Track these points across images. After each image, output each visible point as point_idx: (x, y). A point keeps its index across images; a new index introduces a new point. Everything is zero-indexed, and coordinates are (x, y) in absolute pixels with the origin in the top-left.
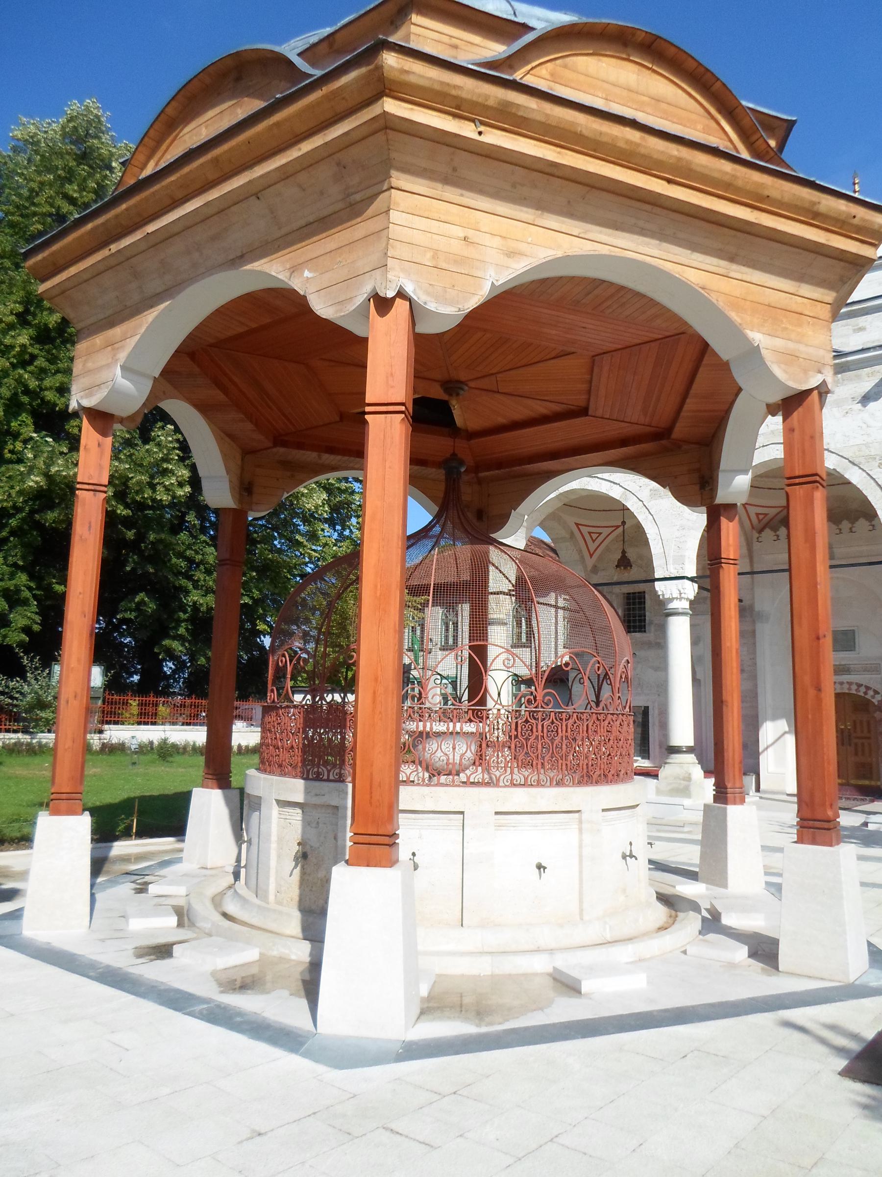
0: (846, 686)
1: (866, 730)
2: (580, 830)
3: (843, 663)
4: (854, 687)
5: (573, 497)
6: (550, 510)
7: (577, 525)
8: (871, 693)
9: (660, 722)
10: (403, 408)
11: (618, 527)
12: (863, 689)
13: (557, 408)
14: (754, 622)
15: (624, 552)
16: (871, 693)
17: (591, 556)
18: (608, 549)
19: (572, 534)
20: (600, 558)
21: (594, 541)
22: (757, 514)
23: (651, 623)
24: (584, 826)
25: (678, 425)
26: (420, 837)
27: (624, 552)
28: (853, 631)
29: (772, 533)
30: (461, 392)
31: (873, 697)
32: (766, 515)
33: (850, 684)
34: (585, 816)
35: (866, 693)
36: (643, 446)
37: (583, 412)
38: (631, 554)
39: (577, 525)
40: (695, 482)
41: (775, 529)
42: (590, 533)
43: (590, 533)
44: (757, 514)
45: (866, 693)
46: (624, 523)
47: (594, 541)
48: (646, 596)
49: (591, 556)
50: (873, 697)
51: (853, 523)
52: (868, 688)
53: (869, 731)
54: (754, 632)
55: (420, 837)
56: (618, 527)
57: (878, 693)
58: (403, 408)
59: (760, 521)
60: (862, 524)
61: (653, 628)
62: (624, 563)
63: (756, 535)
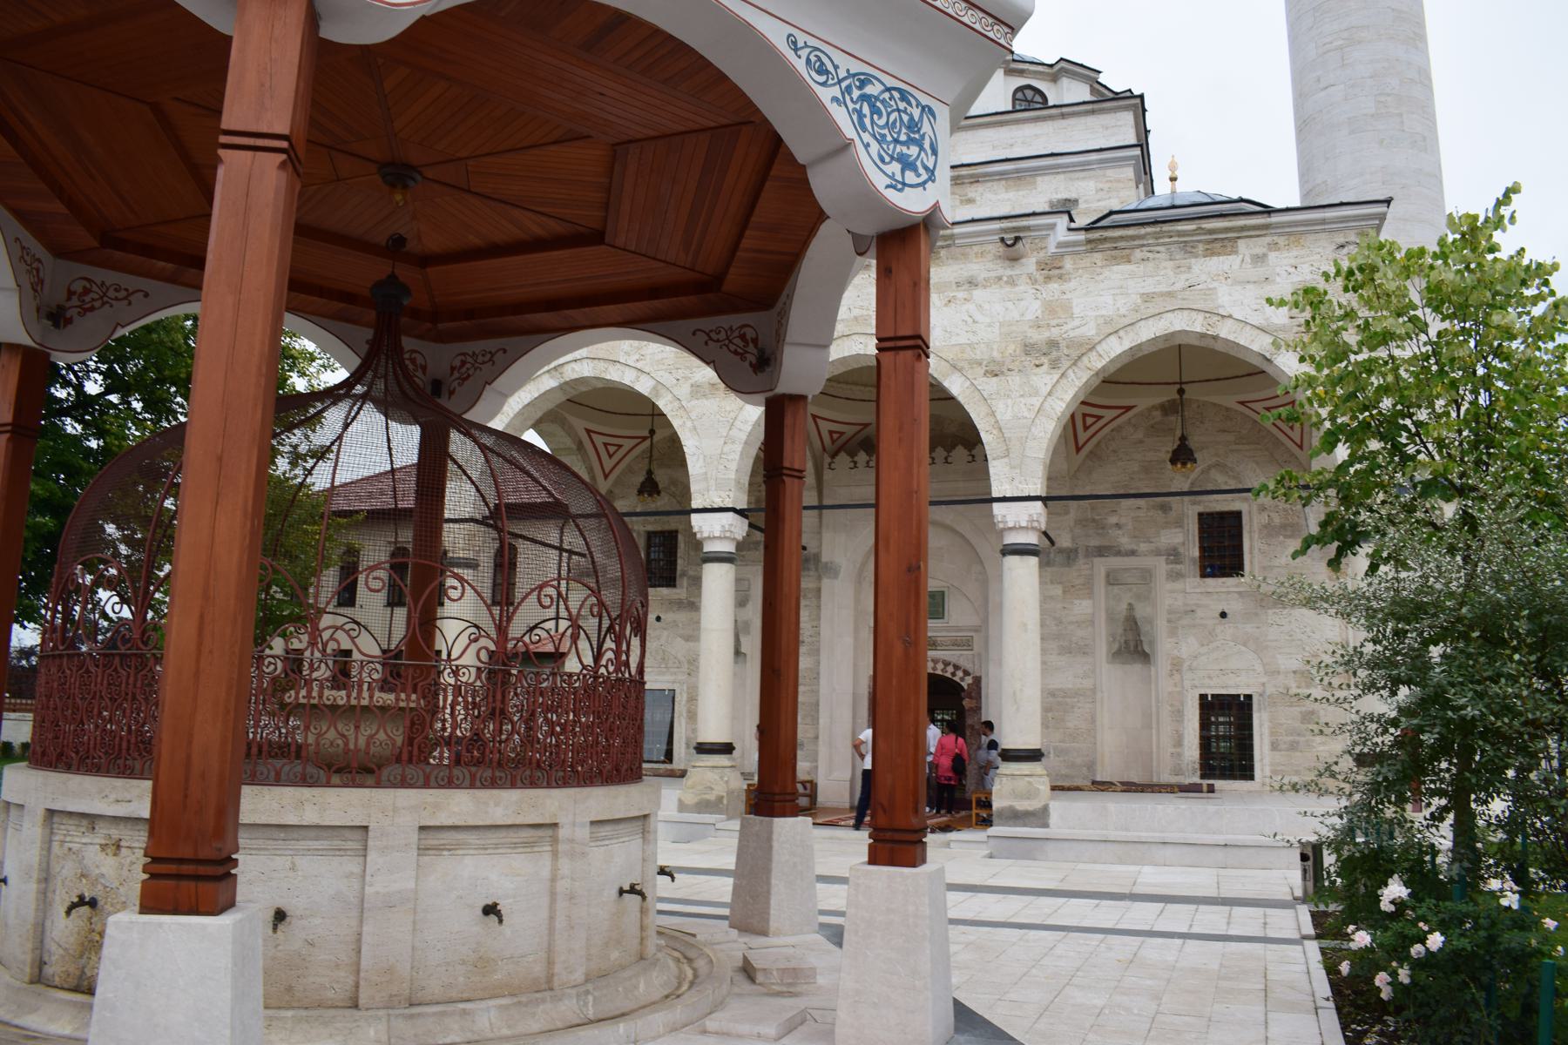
2: (555, 854)
4: (940, 666)
5: (584, 389)
6: (550, 406)
7: (588, 431)
8: (960, 674)
9: (689, 711)
10: (284, 144)
11: (644, 439)
12: (950, 669)
13: (557, 227)
14: (819, 578)
15: (650, 473)
16: (960, 674)
17: (606, 476)
18: (630, 470)
19: (580, 445)
20: (617, 482)
21: (611, 456)
22: (831, 433)
23: (684, 574)
24: (562, 847)
25: (732, 270)
26: (293, 868)
27: (650, 473)
29: (849, 459)
30: (411, 183)
31: (962, 679)
32: (842, 434)
34: (563, 833)
35: (954, 674)
36: (683, 299)
37: (596, 237)
38: (661, 476)
39: (588, 431)
40: (748, 362)
41: (852, 454)
42: (606, 445)
43: (606, 445)
44: (831, 433)
45: (954, 674)
46: (652, 432)
47: (611, 456)
48: (680, 537)
49: (606, 476)
50: (962, 679)
51: (949, 451)
52: (956, 667)
54: (819, 590)
55: (293, 868)
56: (644, 439)
58: (284, 144)
59: (833, 442)
60: (960, 452)
61: (685, 582)
62: (650, 487)
63: (827, 460)
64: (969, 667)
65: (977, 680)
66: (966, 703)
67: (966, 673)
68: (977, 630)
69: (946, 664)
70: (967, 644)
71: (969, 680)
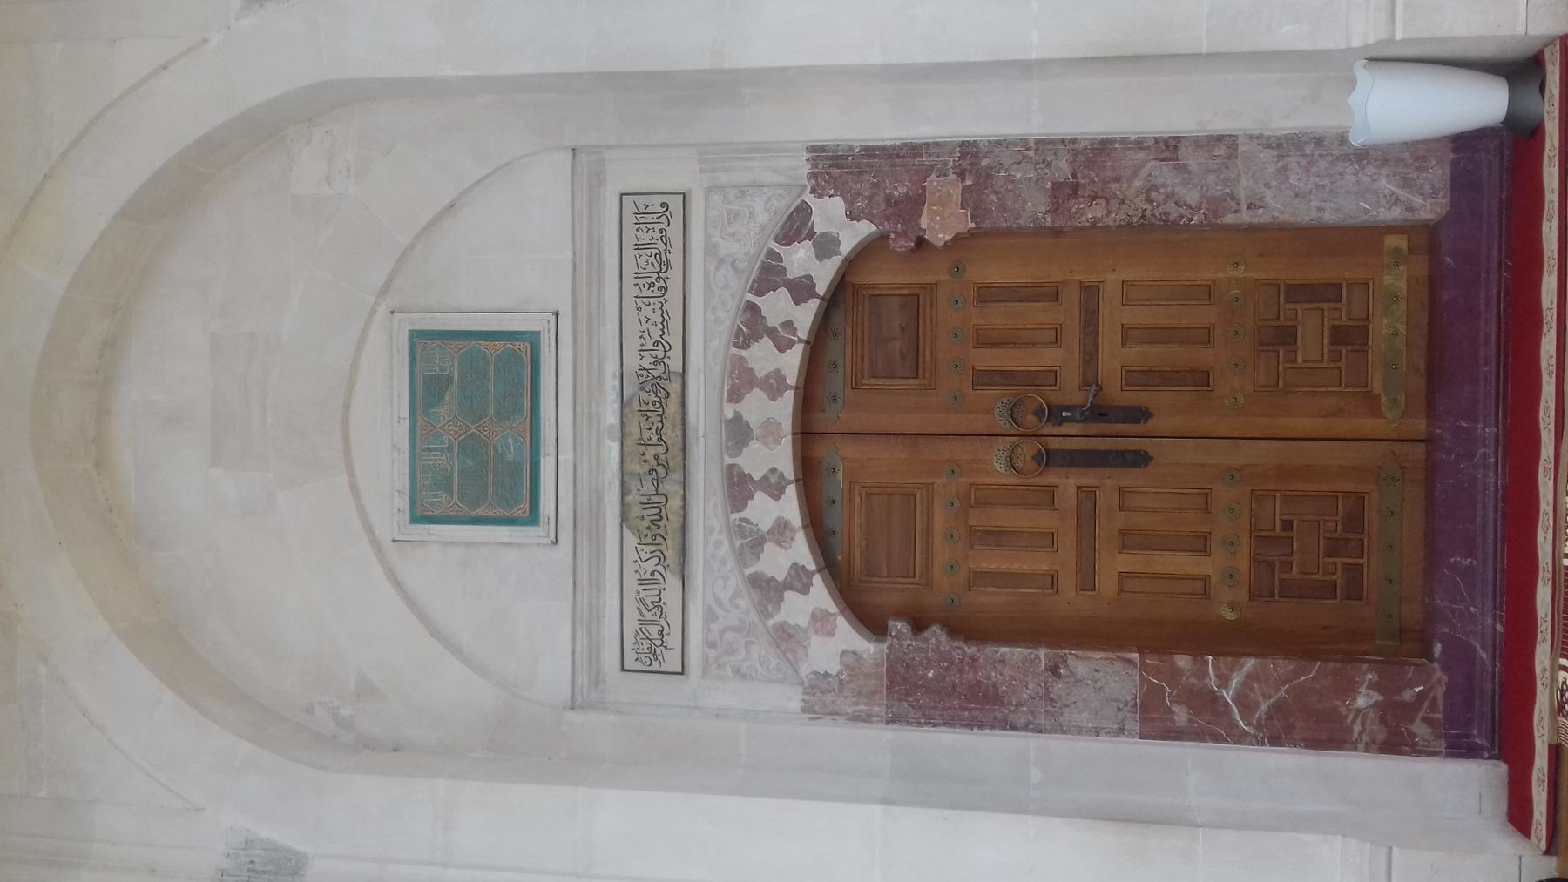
0: (755, 407)
1: (1040, 315)
3: (611, 416)
4: (763, 358)
8: (799, 259)
12: (777, 306)
16: (799, 259)
28: (420, 339)
31: (825, 246)
33: (740, 382)
35: (801, 290)
45: (801, 290)
50: (825, 246)
52: (769, 276)
53: (1053, 294)
57: (804, 211)
64: (765, 213)
65: (835, 167)
66: (942, 223)
67: (796, 226)
68: (587, 167)
69: (752, 326)
70: (656, 228)
71: (829, 213)
